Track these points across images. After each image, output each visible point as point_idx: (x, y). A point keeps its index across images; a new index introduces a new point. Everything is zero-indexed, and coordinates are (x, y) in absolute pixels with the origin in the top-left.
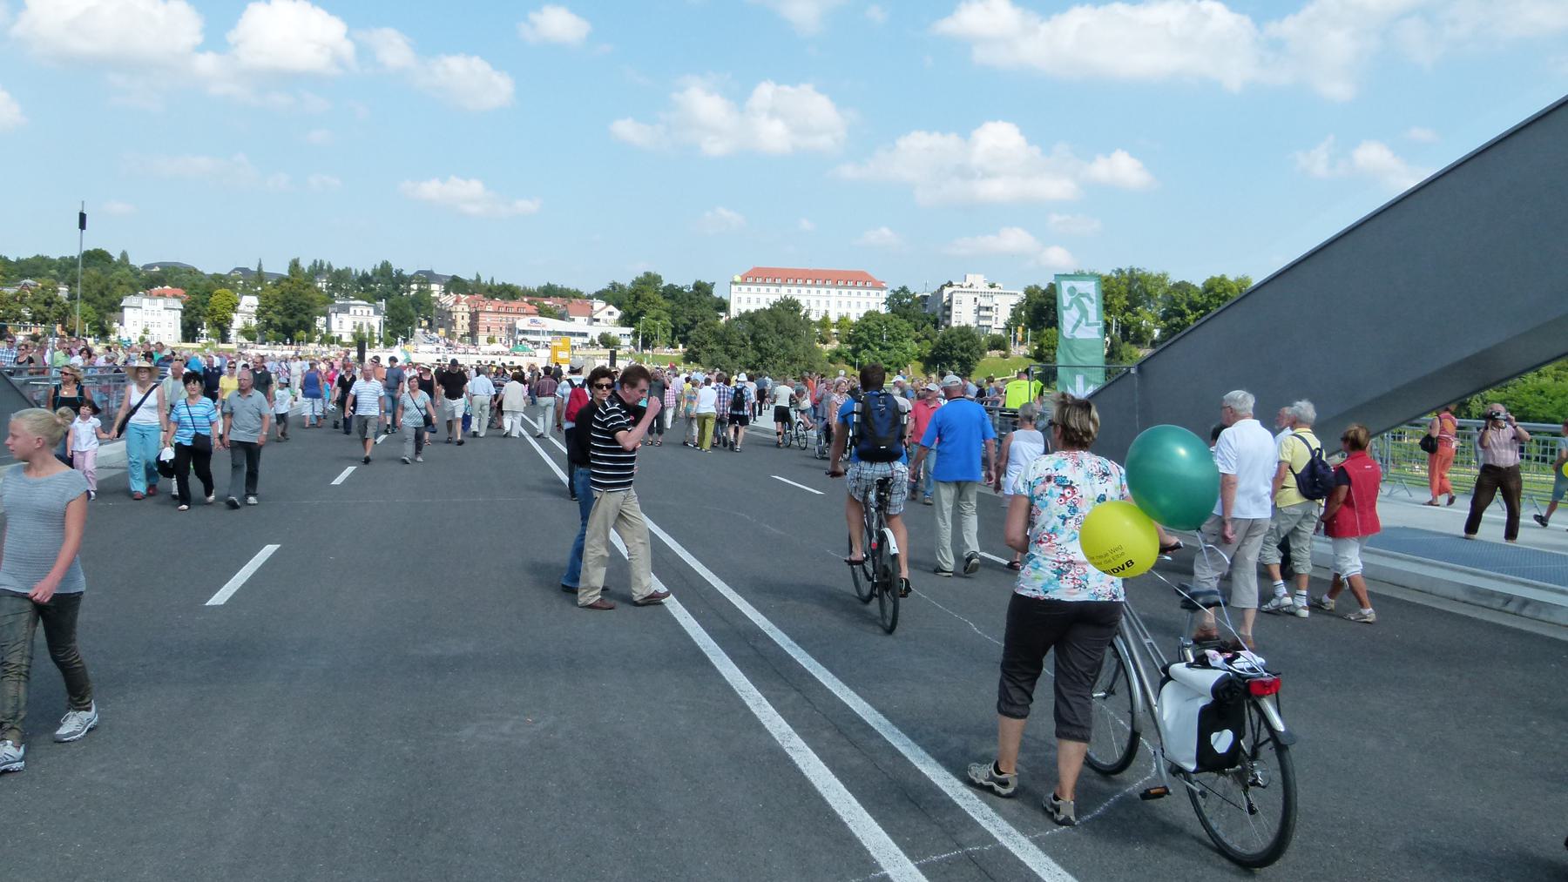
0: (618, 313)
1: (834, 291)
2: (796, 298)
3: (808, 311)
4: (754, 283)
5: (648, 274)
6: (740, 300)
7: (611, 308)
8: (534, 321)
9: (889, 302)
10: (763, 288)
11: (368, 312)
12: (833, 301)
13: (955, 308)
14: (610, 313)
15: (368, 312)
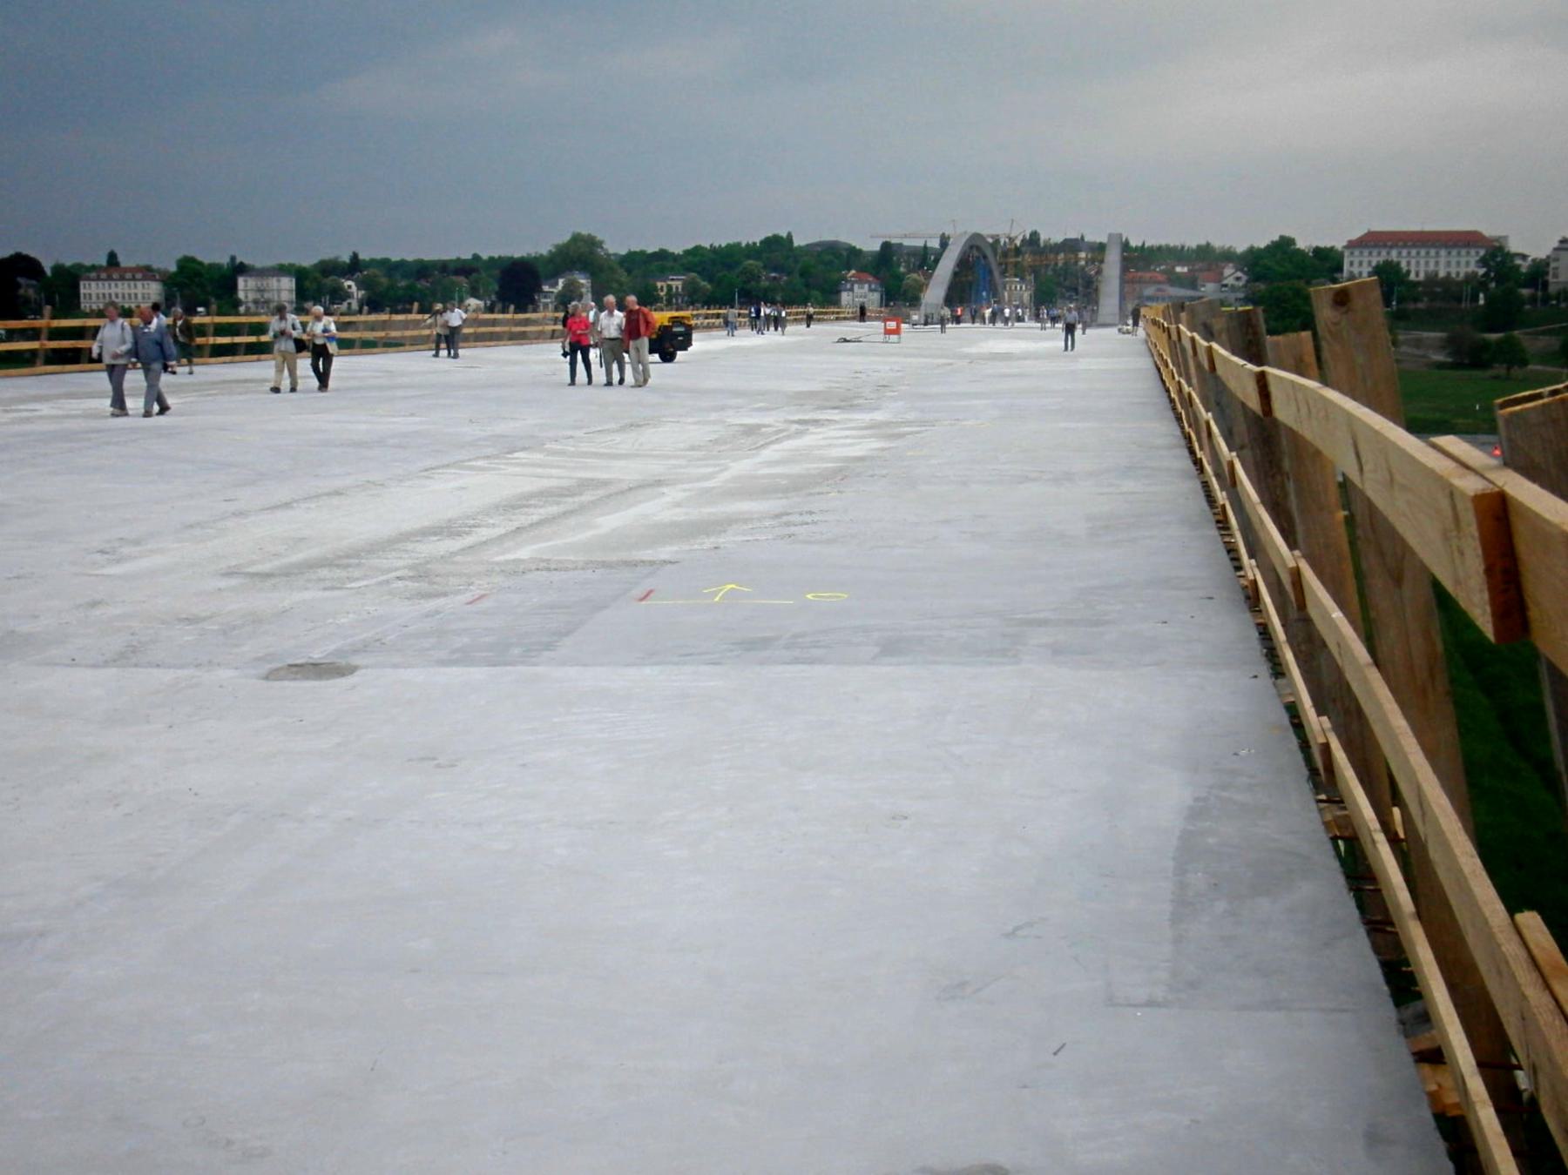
0: (1245, 278)
1: (1443, 252)
2: (1395, 259)
3: (1409, 272)
4: (1366, 246)
5: (1282, 237)
6: (1351, 264)
7: (1239, 274)
8: (1159, 290)
9: (1483, 262)
10: (1375, 253)
11: (1021, 288)
12: (1442, 261)
13: (1553, 265)
14: (1238, 279)
15: (1021, 288)
